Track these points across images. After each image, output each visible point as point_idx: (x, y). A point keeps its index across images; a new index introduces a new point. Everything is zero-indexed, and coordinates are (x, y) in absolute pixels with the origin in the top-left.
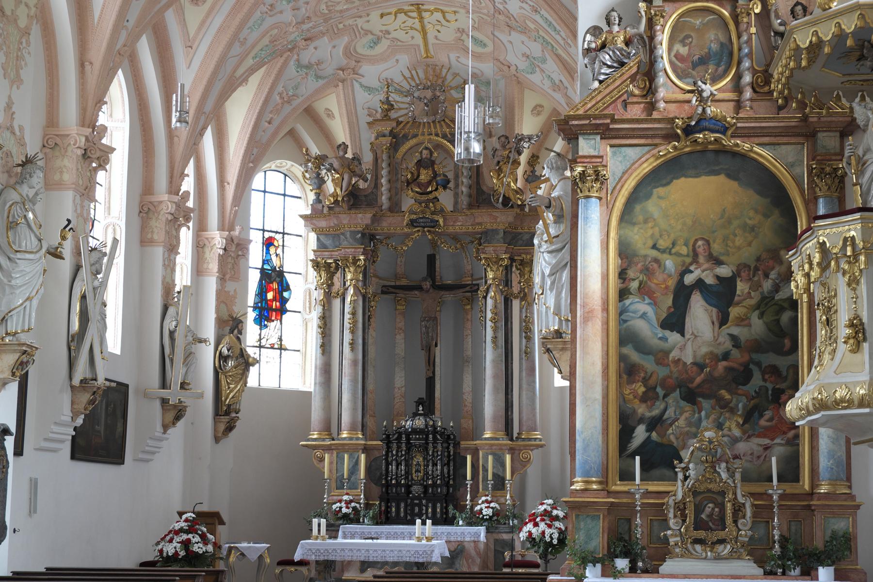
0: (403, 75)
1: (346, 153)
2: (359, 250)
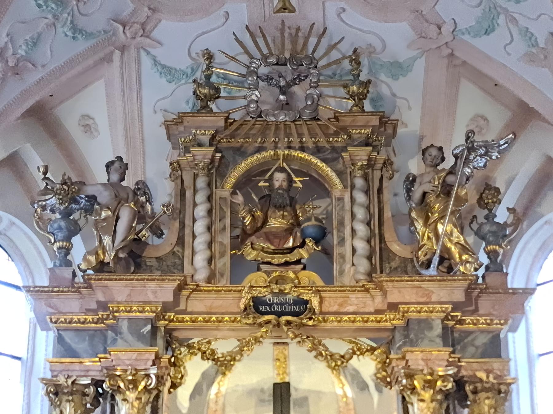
0: (237, 39)
1: (123, 179)
2: (147, 356)
